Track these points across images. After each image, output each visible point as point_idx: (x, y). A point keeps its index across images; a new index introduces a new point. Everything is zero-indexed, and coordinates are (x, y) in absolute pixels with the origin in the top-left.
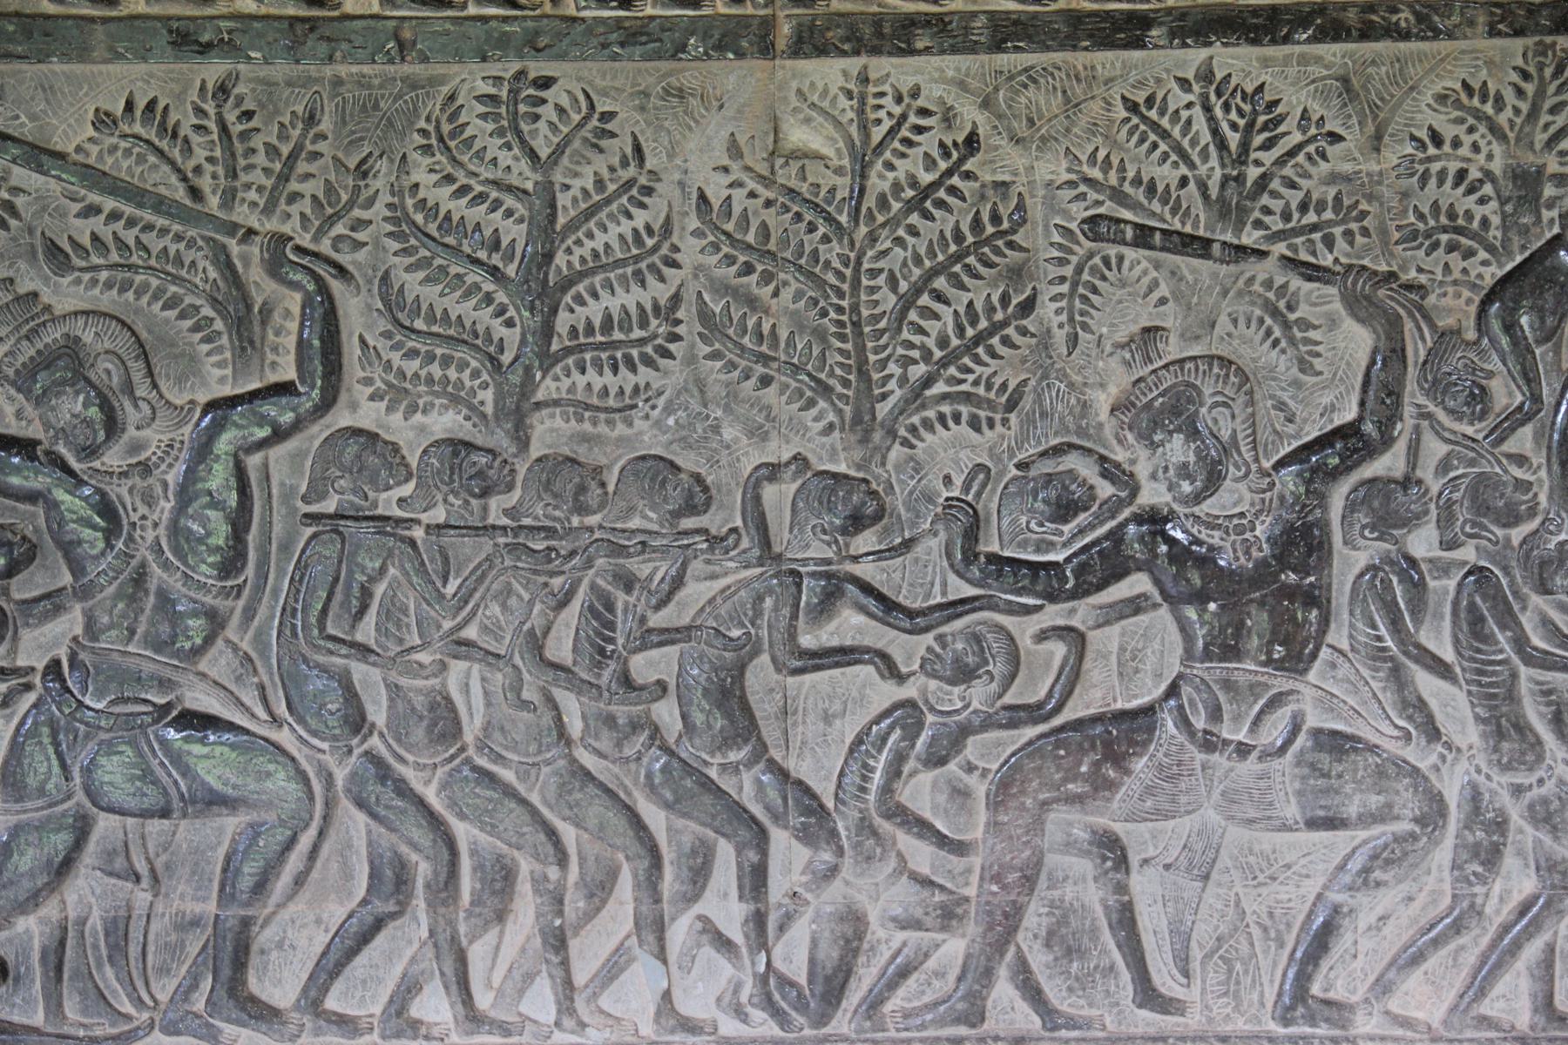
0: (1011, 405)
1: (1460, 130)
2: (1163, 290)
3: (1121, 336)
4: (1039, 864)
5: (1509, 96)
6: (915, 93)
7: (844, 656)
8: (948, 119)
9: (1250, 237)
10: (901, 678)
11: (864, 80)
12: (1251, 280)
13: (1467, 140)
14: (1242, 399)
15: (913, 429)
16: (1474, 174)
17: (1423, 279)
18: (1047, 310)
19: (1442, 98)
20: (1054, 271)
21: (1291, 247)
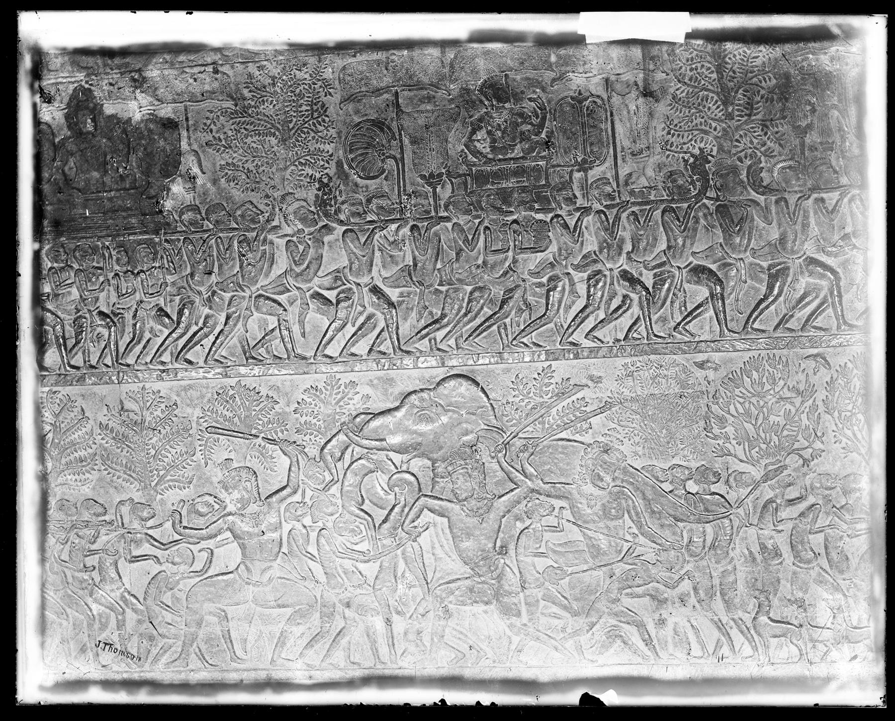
0: (190, 483)
1: (311, 400)
2: (231, 448)
3: (219, 462)
4: (202, 620)
5: (323, 389)
6: (159, 391)
7: (144, 557)
8: (169, 399)
9: (254, 432)
10: (161, 564)
11: (143, 388)
12: (254, 445)
13: (313, 403)
14: (254, 479)
15: (162, 490)
16: (316, 412)
17: (304, 443)
18: (198, 454)
19: (305, 391)
20: (200, 443)
21: (266, 434)
